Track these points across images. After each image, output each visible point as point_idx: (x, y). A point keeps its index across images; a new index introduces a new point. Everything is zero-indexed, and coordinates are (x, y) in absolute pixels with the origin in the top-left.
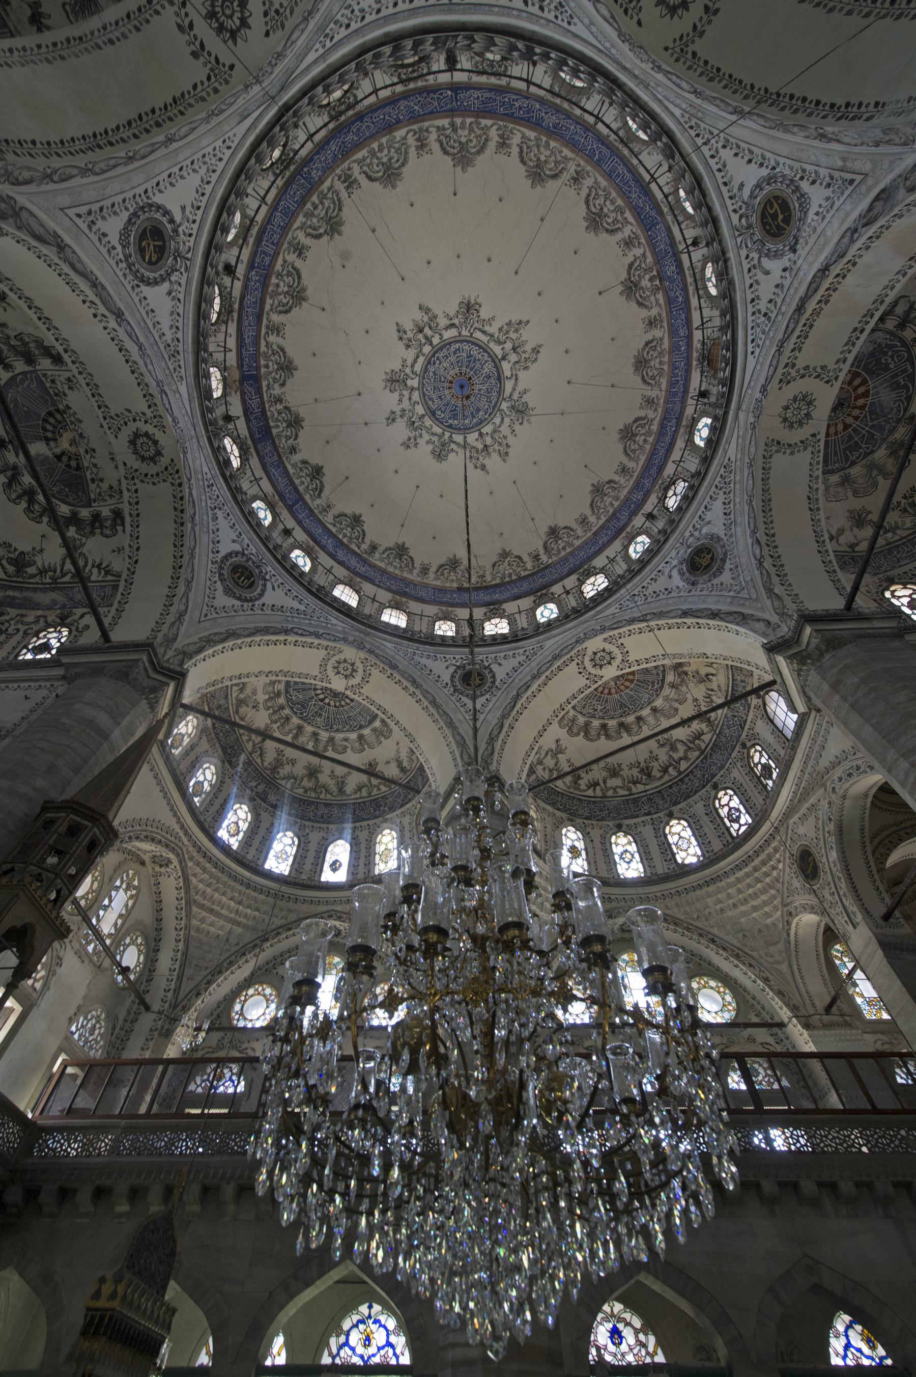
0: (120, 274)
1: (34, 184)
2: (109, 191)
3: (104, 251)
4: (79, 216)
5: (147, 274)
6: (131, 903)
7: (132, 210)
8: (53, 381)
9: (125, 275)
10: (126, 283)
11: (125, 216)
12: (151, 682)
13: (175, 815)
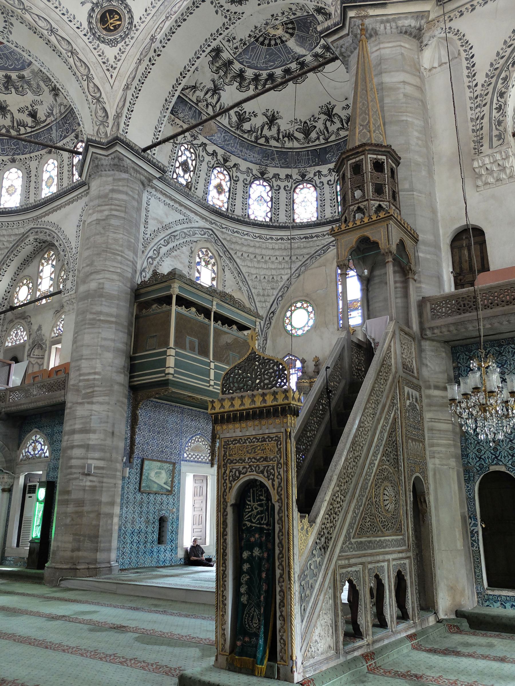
0: (132, 41)
1: (104, 105)
2: (94, 60)
3: (123, 56)
4: (111, 76)
5: (127, 21)
7: (98, 42)
8: (236, 48)
9: (132, 38)
10: (136, 36)
11: (102, 46)
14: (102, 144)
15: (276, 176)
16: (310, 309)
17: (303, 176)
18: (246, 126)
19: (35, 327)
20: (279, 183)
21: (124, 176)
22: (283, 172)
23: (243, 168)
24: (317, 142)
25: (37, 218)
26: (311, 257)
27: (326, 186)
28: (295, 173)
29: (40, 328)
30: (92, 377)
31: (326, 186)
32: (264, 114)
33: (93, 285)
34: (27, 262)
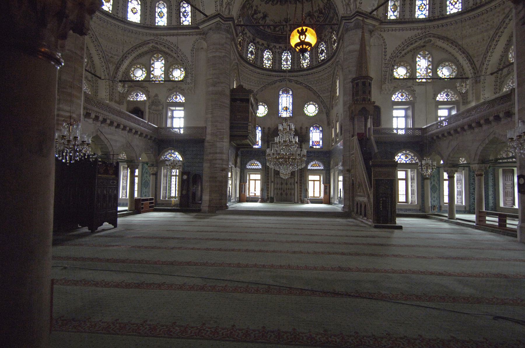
6: (430, 59)
12: (353, 23)
13: (414, 29)
14: (223, 17)
15: (258, 42)
16: (266, 106)
17: (269, 46)
18: (255, 16)
19: (152, 94)
20: (259, 46)
21: (229, 36)
22: (261, 42)
23: (248, 35)
24: (278, 33)
25: (157, 35)
26: (268, 84)
27: (277, 54)
28: (265, 43)
29: (156, 95)
30: (222, 131)
31: (277, 54)
32: (263, 13)
33: (220, 89)
34: (140, 56)
